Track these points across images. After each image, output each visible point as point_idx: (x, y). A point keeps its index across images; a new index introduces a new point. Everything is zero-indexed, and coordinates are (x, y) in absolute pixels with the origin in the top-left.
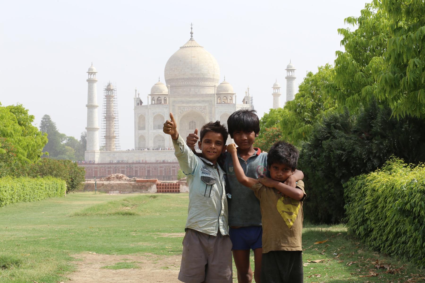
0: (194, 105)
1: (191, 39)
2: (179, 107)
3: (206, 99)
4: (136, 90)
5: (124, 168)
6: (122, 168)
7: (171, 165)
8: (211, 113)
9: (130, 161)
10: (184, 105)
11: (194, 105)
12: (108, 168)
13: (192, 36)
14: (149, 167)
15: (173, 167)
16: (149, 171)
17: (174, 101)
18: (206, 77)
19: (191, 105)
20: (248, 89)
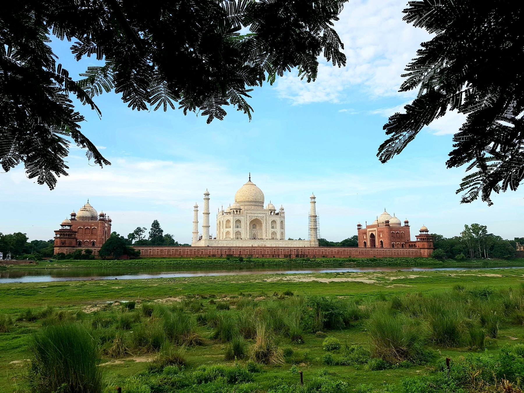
1: (250, 181)
16: (240, 252)
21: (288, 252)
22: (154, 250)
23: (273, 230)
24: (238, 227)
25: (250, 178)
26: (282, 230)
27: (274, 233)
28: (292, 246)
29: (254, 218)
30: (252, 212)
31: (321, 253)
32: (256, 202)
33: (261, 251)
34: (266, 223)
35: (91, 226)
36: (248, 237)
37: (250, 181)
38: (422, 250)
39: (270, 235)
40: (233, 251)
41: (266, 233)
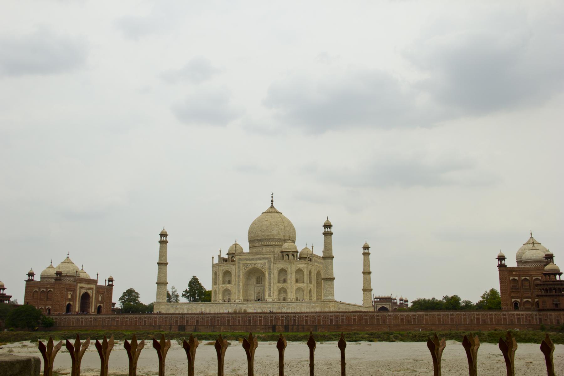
0: (256, 262)
1: (272, 206)
2: (244, 264)
3: (266, 256)
4: (220, 251)
5: (178, 317)
6: (176, 317)
7: (216, 316)
8: (270, 269)
9: (190, 312)
10: (248, 262)
11: (256, 262)
12: (165, 318)
13: (272, 204)
14: (198, 317)
15: (217, 317)
16: (197, 321)
17: (240, 259)
18: (276, 237)
19: (253, 262)
20: (313, 247)
21: (271, 320)
22: (86, 318)
23: (281, 285)
24: (230, 282)
25: (272, 201)
26: (299, 285)
27: (283, 291)
28: (288, 311)
29: (250, 267)
30: (247, 257)
31: (328, 322)
32: (270, 240)
33: (228, 320)
34: (269, 274)
35: (47, 288)
36: (241, 298)
37: (272, 206)
38: (542, 313)
39: (276, 293)
40: (187, 321)
41: (270, 290)
